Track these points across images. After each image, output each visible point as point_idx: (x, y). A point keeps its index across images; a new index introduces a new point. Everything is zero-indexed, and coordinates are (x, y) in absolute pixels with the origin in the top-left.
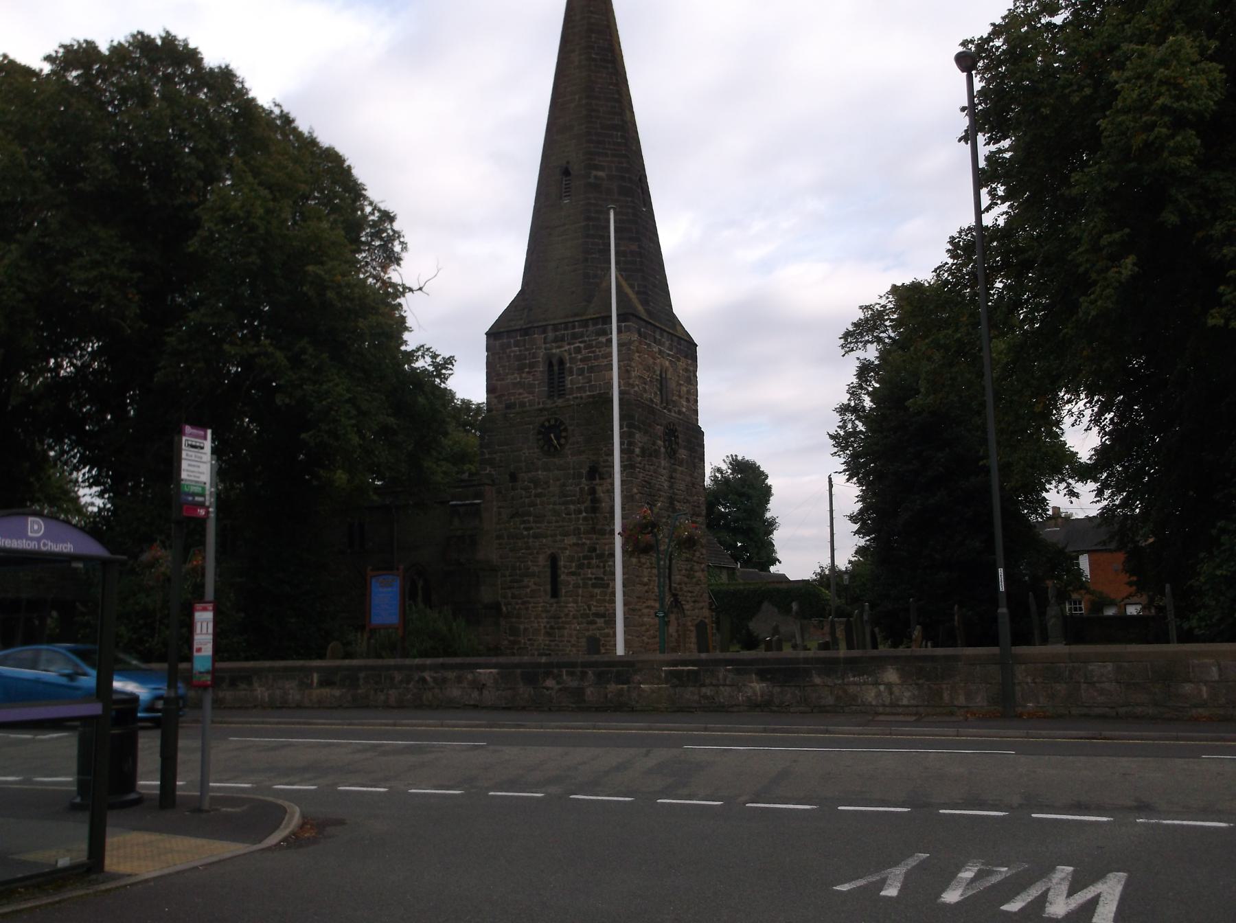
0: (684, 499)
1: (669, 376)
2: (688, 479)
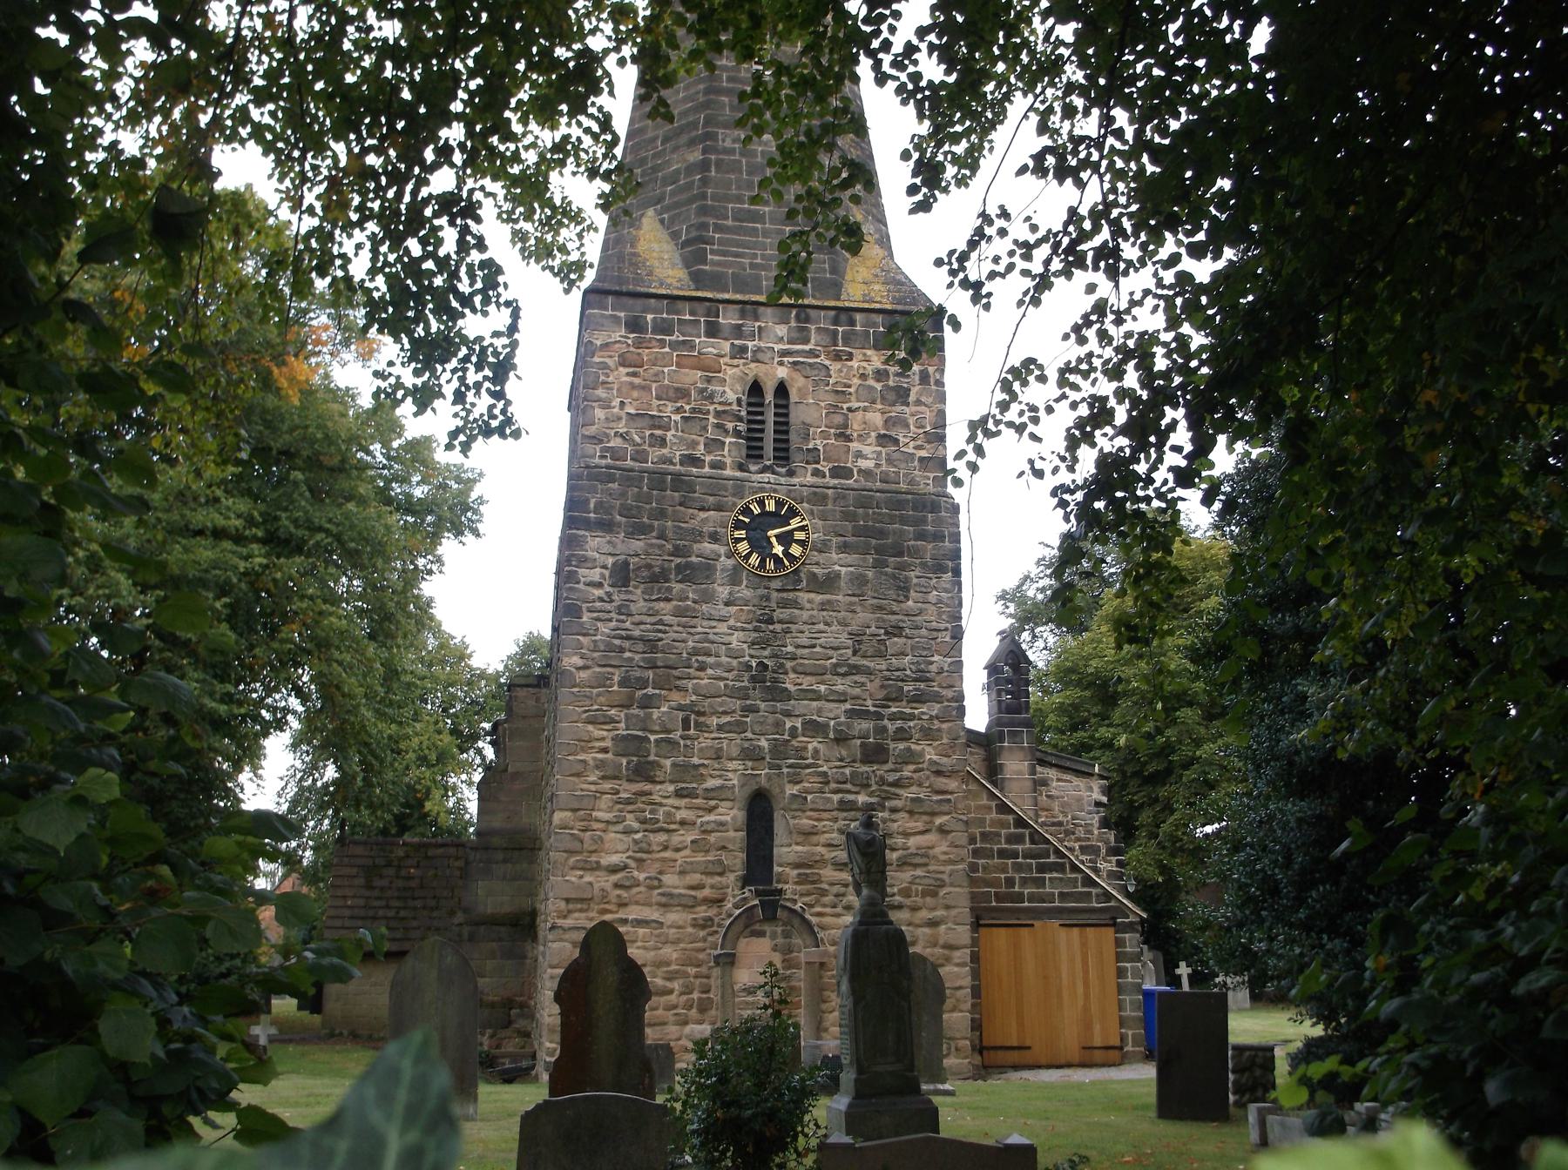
0: (835, 666)
1: (794, 397)
2: (863, 616)
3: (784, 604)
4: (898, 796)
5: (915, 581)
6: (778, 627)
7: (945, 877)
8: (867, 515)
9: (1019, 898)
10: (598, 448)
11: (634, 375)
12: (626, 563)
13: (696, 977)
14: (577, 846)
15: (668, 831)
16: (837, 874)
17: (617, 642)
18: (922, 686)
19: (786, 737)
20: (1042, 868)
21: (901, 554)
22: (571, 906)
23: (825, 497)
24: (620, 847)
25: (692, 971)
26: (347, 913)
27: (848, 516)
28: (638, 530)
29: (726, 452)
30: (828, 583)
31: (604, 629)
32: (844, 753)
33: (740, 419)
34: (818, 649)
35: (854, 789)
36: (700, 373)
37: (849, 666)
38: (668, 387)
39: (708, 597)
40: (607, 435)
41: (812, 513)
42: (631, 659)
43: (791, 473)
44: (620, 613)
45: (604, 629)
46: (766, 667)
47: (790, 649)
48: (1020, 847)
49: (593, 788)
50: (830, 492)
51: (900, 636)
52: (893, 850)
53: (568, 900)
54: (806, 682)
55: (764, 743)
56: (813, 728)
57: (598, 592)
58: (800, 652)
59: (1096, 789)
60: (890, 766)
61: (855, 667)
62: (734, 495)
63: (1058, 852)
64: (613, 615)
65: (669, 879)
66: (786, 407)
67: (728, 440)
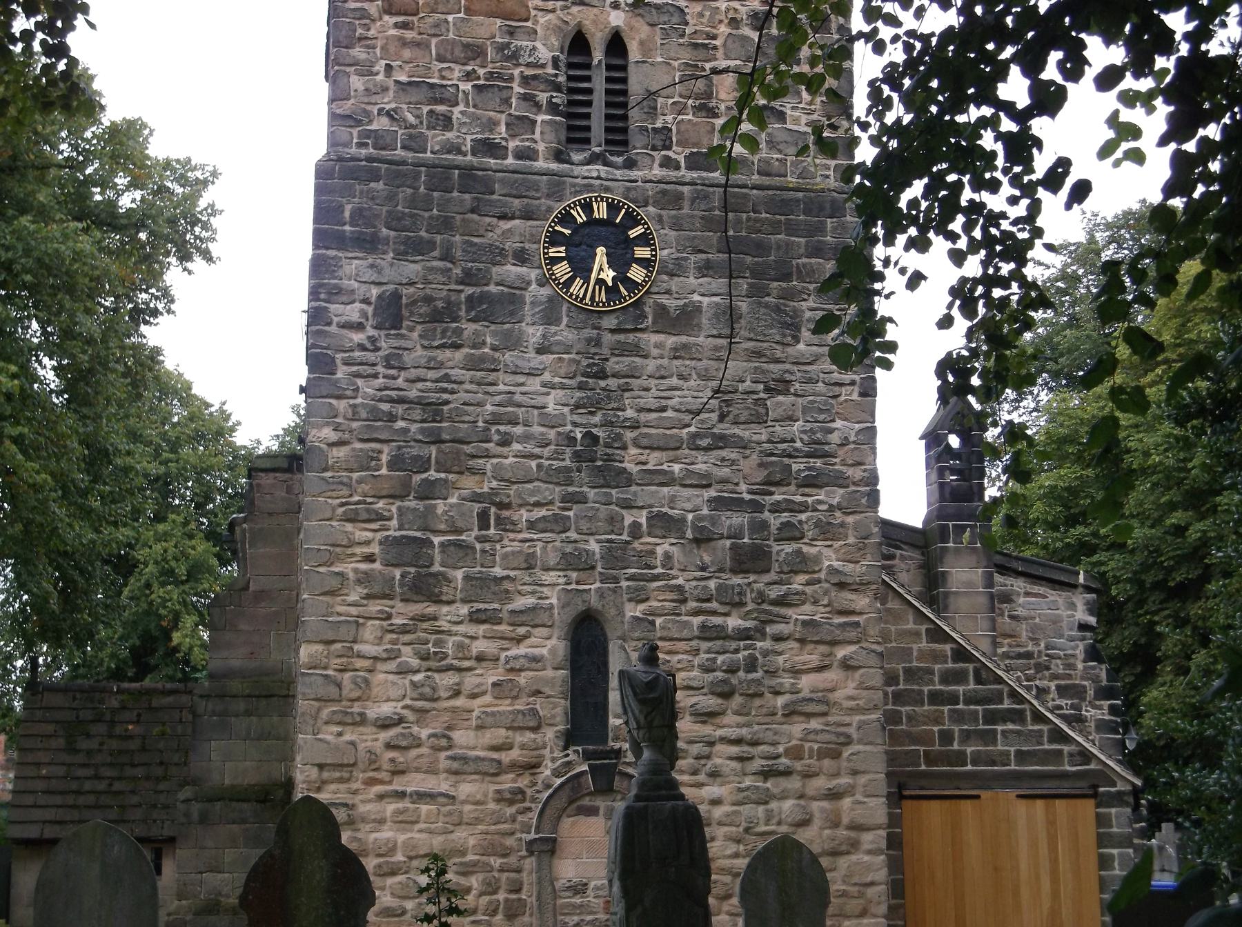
0: (694, 436)
1: (634, 53)
3: (621, 350)
4: (785, 619)
5: (808, 314)
6: (612, 383)
7: (852, 731)
8: (739, 221)
9: (960, 758)
10: (355, 132)
11: (405, 26)
12: (396, 296)
13: (502, 870)
14: (333, 691)
15: (460, 670)
16: (697, 727)
17: (385, 407)
18: (819, 463)
19: (625, 537)
20: (992, 718)
21: (787, 277)
22: (326, 775)
23: (679, 197)
24: (395, 693)
25: (496, 862)
26: (40, 785)
27: (709, 224)
28: (412, 248)
29: (537, 136)
30: (685, 319)
31: (368, 388)
32: (707, 559)
33: (557, 88)
34: (670, 413)
35: (722, 609)
36: (499, 22)
37: (714, 436)
38: (454, 42)
39: (512, 342)
40: (367, 113)
41: (660, 219)
42: (405, 431)
43: (630, 164)
44: (389, 366)
45: (368, 388)
46: (595, 439)
47: (630, 413)
48: (961, 689)
49: (354, 611)
50: (686, 189)
51: (786, 392)
52: (778, 693)
53: (321, 767)
54: (654, 459)
55: (594, 546)
56: (665, 524)
57: (358, 337)
58: (644, 417)
59: (1081, 607)
60: (773, 576)
61: (722, 437)
62: (548, 196)
63: (1014, 695)
64: (380, 369)
65: (461, 737)
66: (624, 68)
67: (540, 118)
